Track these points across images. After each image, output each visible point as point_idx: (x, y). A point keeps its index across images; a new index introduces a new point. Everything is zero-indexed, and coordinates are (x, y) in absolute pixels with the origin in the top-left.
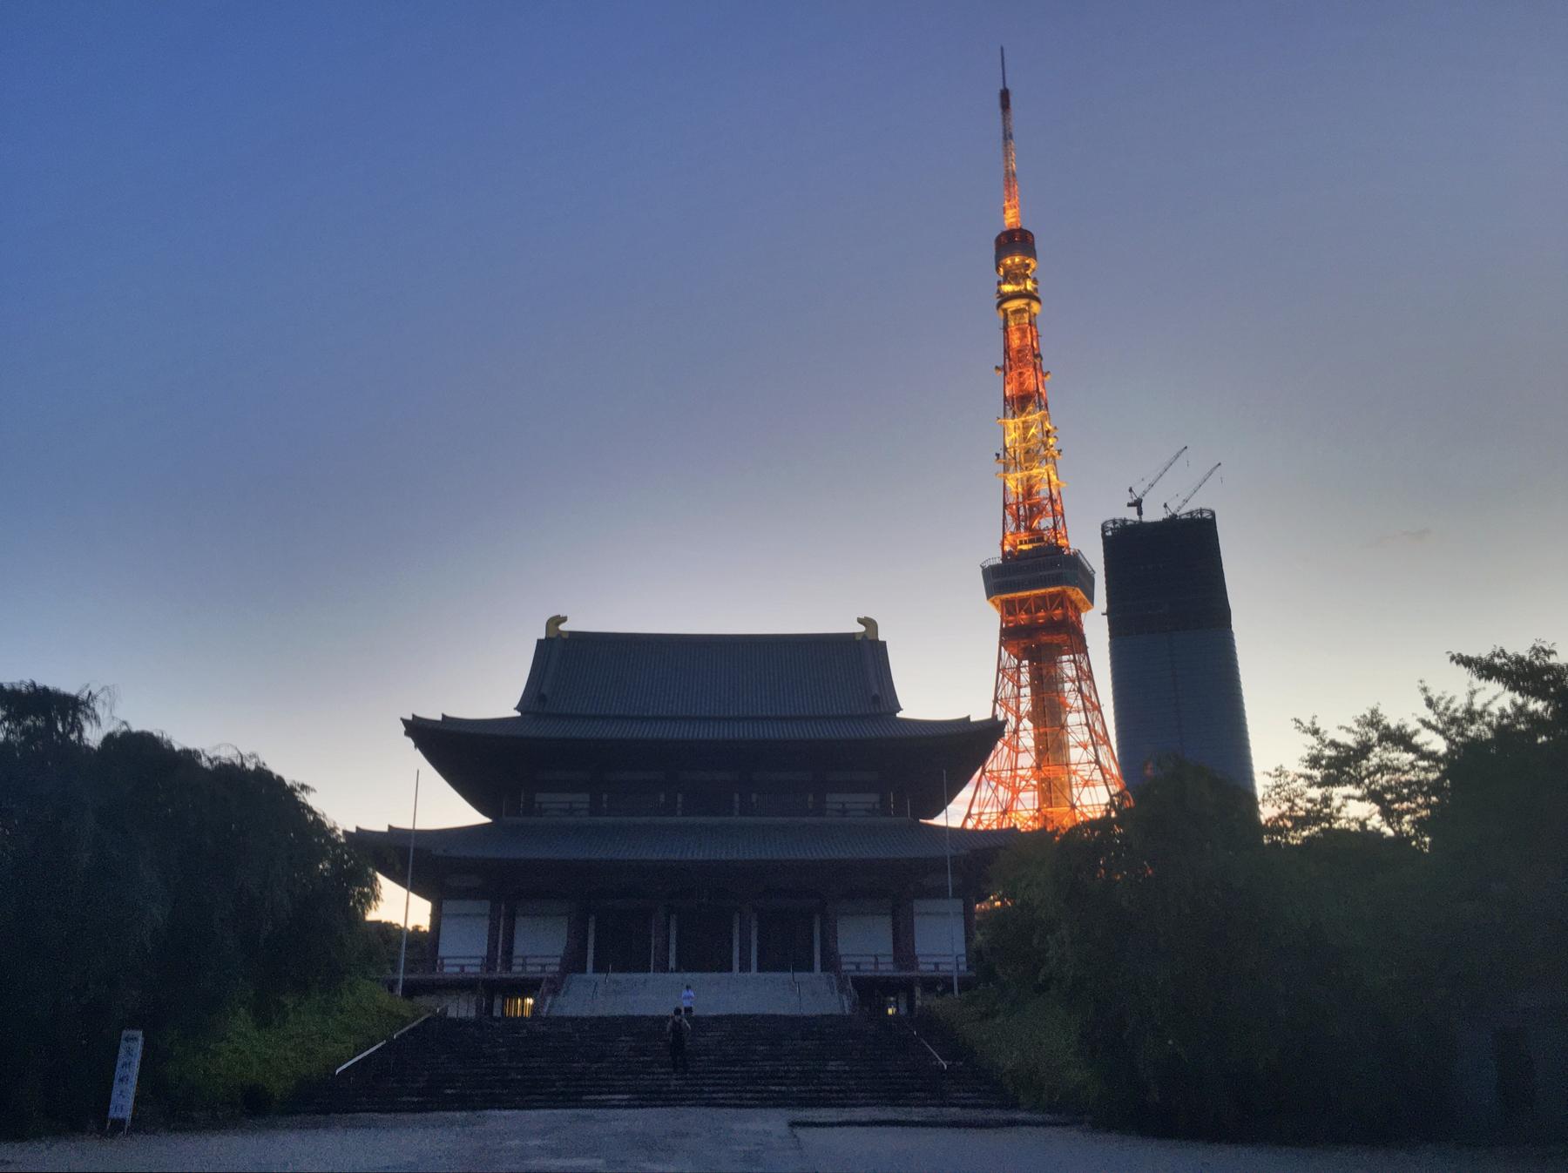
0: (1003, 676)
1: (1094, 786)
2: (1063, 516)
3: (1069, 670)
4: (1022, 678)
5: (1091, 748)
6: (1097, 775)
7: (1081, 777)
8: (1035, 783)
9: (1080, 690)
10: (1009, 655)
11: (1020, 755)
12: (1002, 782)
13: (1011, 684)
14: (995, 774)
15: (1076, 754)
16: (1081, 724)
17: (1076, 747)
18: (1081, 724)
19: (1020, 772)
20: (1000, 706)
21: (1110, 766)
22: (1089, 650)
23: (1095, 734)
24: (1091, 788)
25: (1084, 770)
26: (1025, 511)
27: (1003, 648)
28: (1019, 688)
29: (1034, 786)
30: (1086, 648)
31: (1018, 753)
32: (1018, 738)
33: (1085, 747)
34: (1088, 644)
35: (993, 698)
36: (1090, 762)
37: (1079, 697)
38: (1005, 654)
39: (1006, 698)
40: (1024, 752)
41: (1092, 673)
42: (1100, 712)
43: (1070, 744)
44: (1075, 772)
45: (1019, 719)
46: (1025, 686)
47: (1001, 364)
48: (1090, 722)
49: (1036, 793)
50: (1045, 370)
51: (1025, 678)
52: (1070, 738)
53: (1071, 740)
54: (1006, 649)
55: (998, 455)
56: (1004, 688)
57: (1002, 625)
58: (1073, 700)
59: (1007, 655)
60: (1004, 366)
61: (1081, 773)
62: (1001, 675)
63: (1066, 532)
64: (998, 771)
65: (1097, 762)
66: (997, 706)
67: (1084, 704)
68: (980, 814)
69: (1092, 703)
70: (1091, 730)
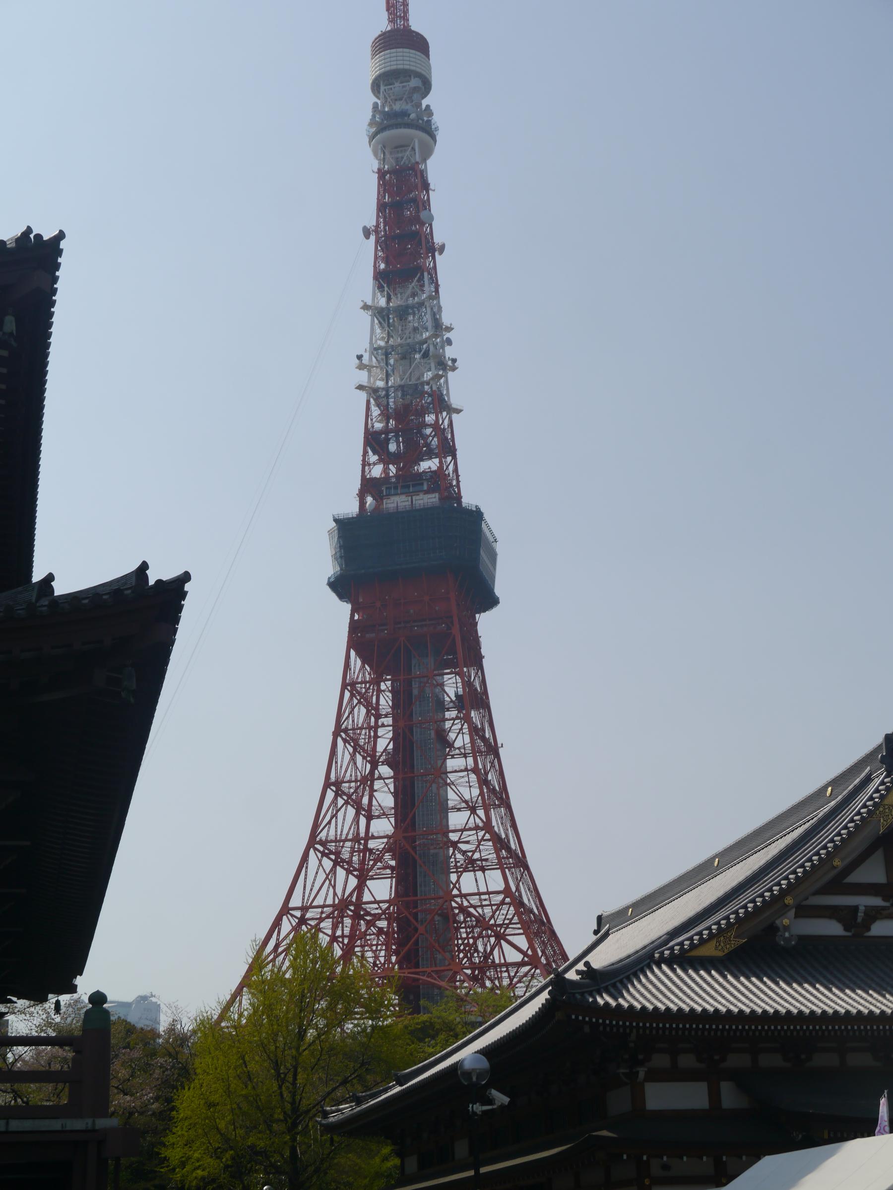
0: (352, 696)
1: (483, 869)
2: (454, 457)
3: (452, 686)
4: (382, 701)
5: (481, 813)
6: (488, 851)
7: (464, 853)
8: (393, 863)
9: (467, 719)
10: (363, 667)
11: (374, 823)
12: (343, 861)
13: (363, 711)
14: (332, 847)
15: (456, 819)
16: (466, 770)
17: (459, 810)
18: (466, 770)
19: (372, 844)
20: (345, 741)
21: (507, 835)
22: (485, 663)
23: (488, 788)
24: (479, 874)
25: (468, 842)
26: (398, 446)
27: (353, 653)
28: (378, 716)
29: (392, 868)
30: (482, 657)
31: (369, 818)
32: (372, 790)
33: (473, 810)
34: (484, 651)
35: (332, 728)
36: (477, 828)
37: (466, 730)
38: (356, 662)
39: (353, 729)
40: (378, 817)
41: (487, 698)
42: (497, 755)
43: (451, 804)
44: (455, 844)
45: (374, 765)
46: (386, 716)
47: (371, 222)
48: (480, 767)
49: (394, 879)
50: (438, 239)
51: (385, 702)
52: (451, 795)
53: (452, 798)
54: (358, 654)
55: (360, 357)
56: (351, 712)
57: (352, 616)
58: (461, 739)
59: (359, 662)
60: (377, 226)
61: (463, 847)
62: (347, 694)
63: (458, 482)
64: (336, 841)
65: (487, 826)
66: (339, 740)
67: (472, 741)
68: (304, 909)
69: (483, 739)
70: (483, 782)
